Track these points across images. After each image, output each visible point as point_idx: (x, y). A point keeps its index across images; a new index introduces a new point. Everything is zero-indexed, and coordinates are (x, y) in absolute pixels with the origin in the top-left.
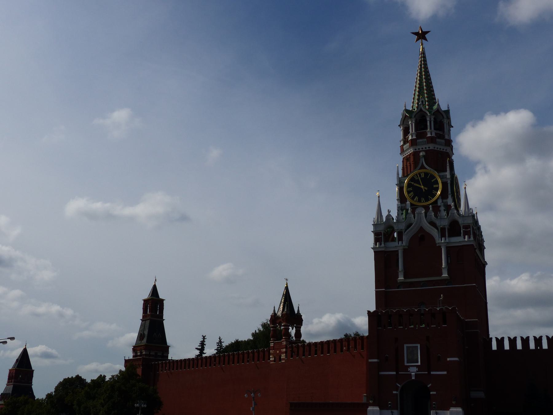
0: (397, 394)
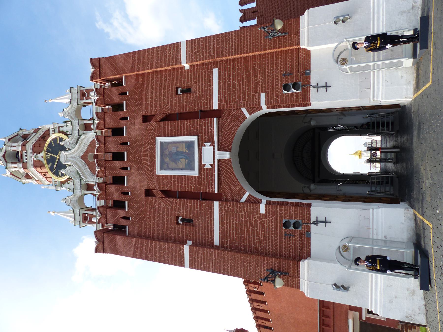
0: (268, 203)
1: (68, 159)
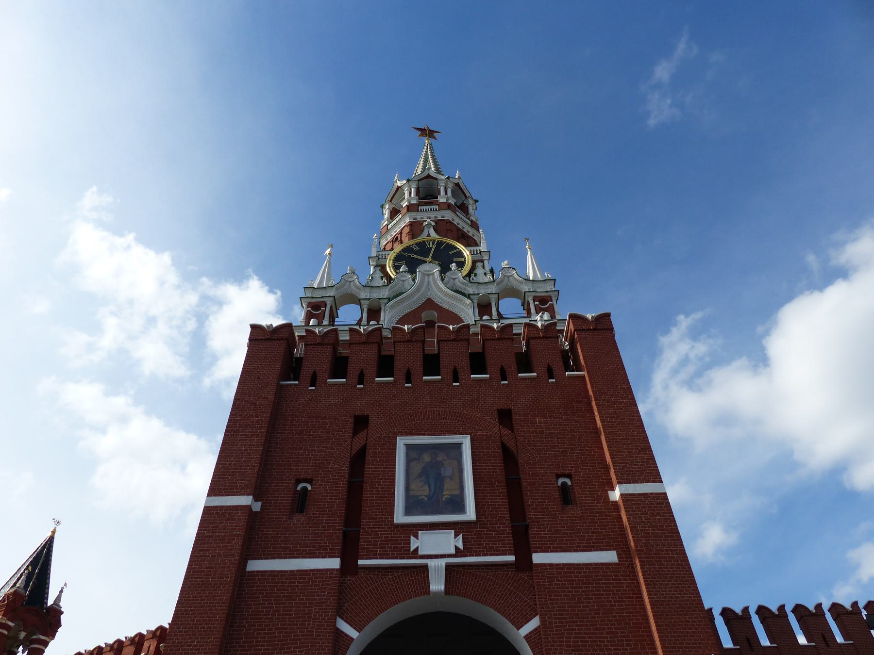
1: (426, 277)
